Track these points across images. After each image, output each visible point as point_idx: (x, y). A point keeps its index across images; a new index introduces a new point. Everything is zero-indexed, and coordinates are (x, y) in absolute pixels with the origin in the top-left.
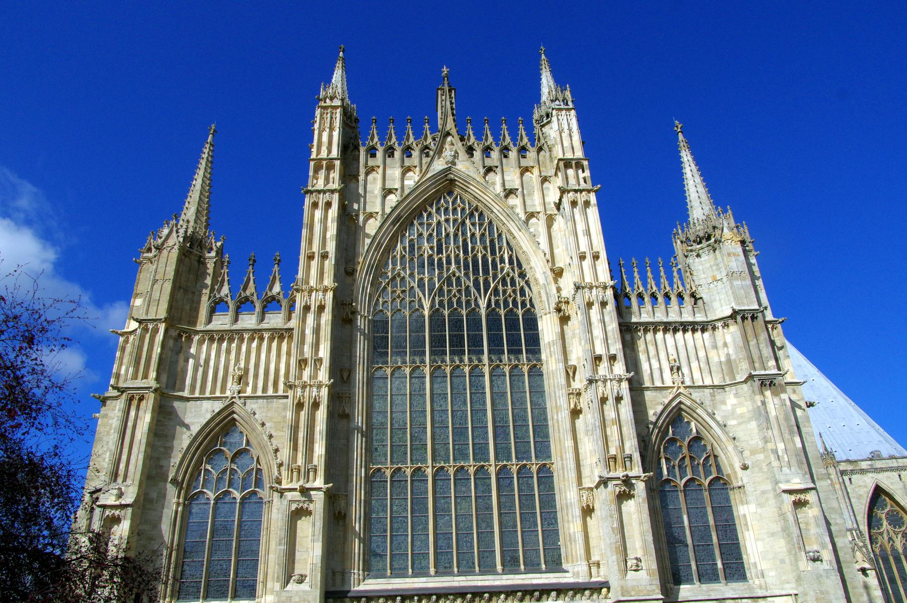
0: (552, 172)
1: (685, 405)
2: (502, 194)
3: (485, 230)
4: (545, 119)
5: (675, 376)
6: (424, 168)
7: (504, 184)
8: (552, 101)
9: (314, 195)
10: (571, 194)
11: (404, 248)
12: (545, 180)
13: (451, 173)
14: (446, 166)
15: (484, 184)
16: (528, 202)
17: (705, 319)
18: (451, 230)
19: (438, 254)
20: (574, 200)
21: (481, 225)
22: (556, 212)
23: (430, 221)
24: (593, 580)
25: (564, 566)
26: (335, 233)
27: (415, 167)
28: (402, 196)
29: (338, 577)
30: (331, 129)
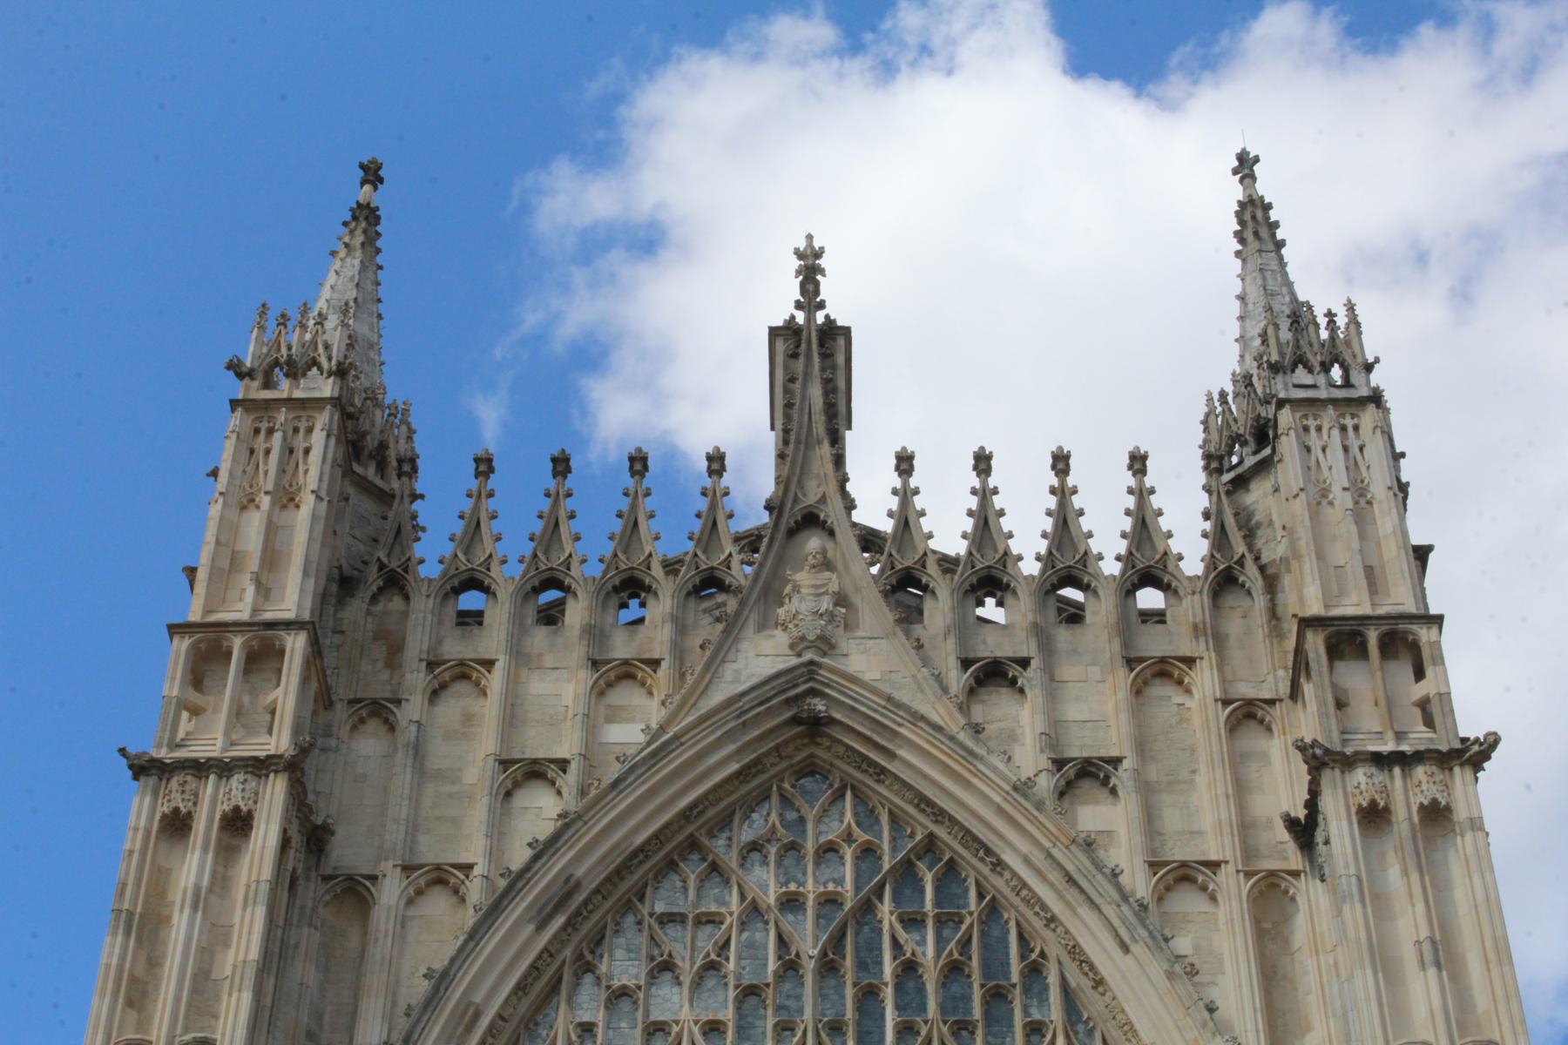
0: (1274, 682)
2: (1046, 784)
3: (965, 944)
6: (697, 661)
8: (1275, 368)
9: (174, 784)
10: (1360, 775)
13: (813, 692)
14: (794, 661)
15: (962, 736)
16: (1171, 820)
18: (808, 943)
20: (1373, 803)
22: (1295, 860)
23: (713, 908)
26: (254, 954)
27: (655, 663)
28: (583, 792)
30: (286, 498)
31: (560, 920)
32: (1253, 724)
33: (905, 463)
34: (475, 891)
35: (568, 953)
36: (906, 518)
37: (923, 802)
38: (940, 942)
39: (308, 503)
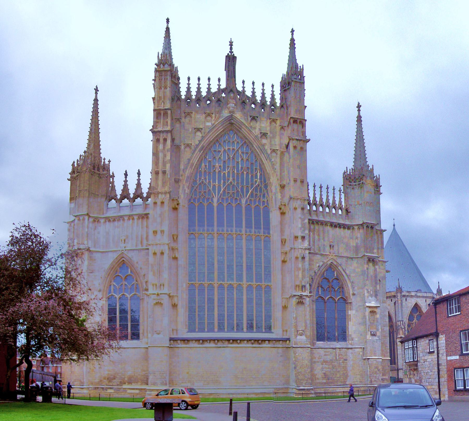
0: (286, 124)
1: (334, 264)
2: (259, 136)
4: (287, 86)
5: (332, 250)
7: (260, 129)
10: (294, 141)
11: (206, 166)
12: (282, 128)
19: (223, 171)
24: (284, 337)
25: (272, 330)
27: (212, 113)
29: (175, 332)
31: (202, 151)
32: (283, 129)
33: (243, 82)
34: (193, 148)
35: (203, 156)
36: (244, 91)
37: (245, 137)
38: (246, 156)
39: (168, 89)
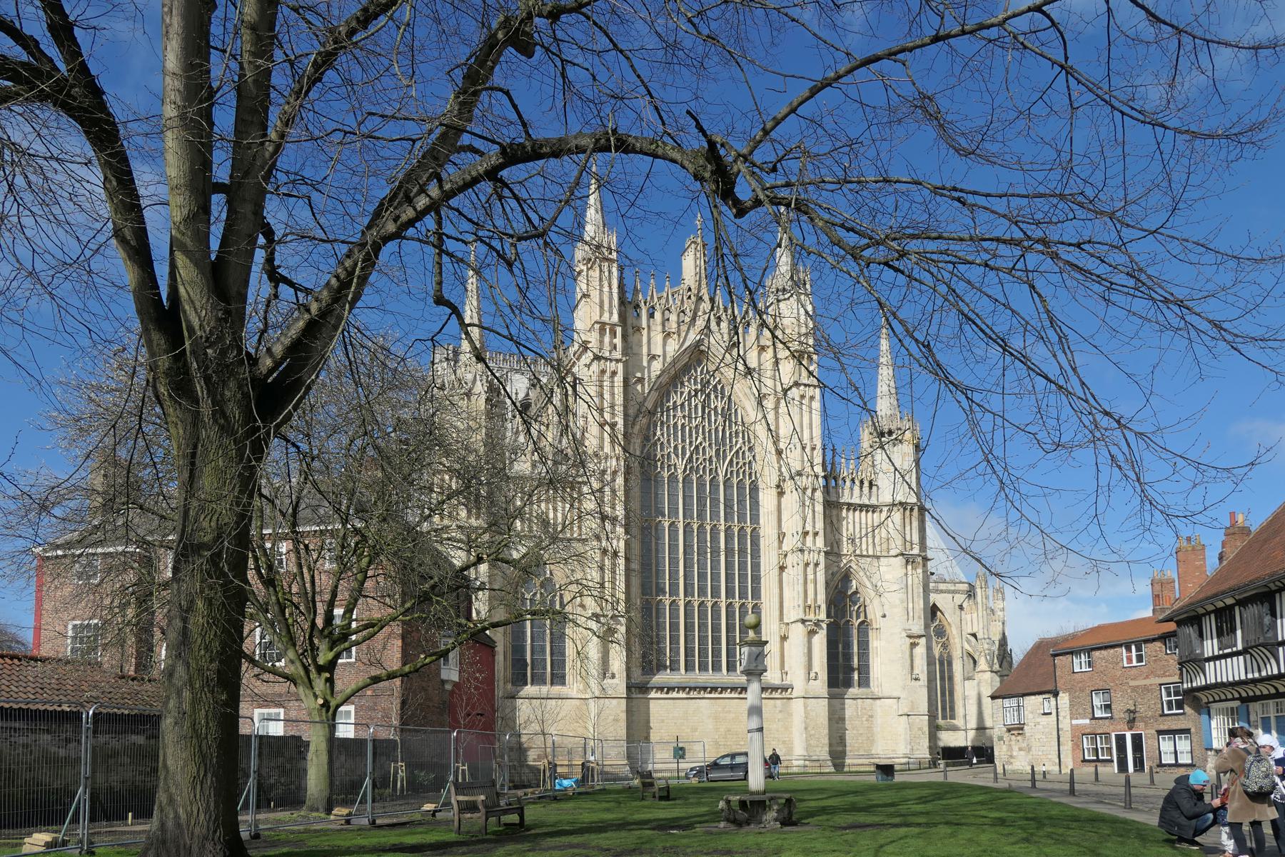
17: (876, 503)
21: (722, 398)
